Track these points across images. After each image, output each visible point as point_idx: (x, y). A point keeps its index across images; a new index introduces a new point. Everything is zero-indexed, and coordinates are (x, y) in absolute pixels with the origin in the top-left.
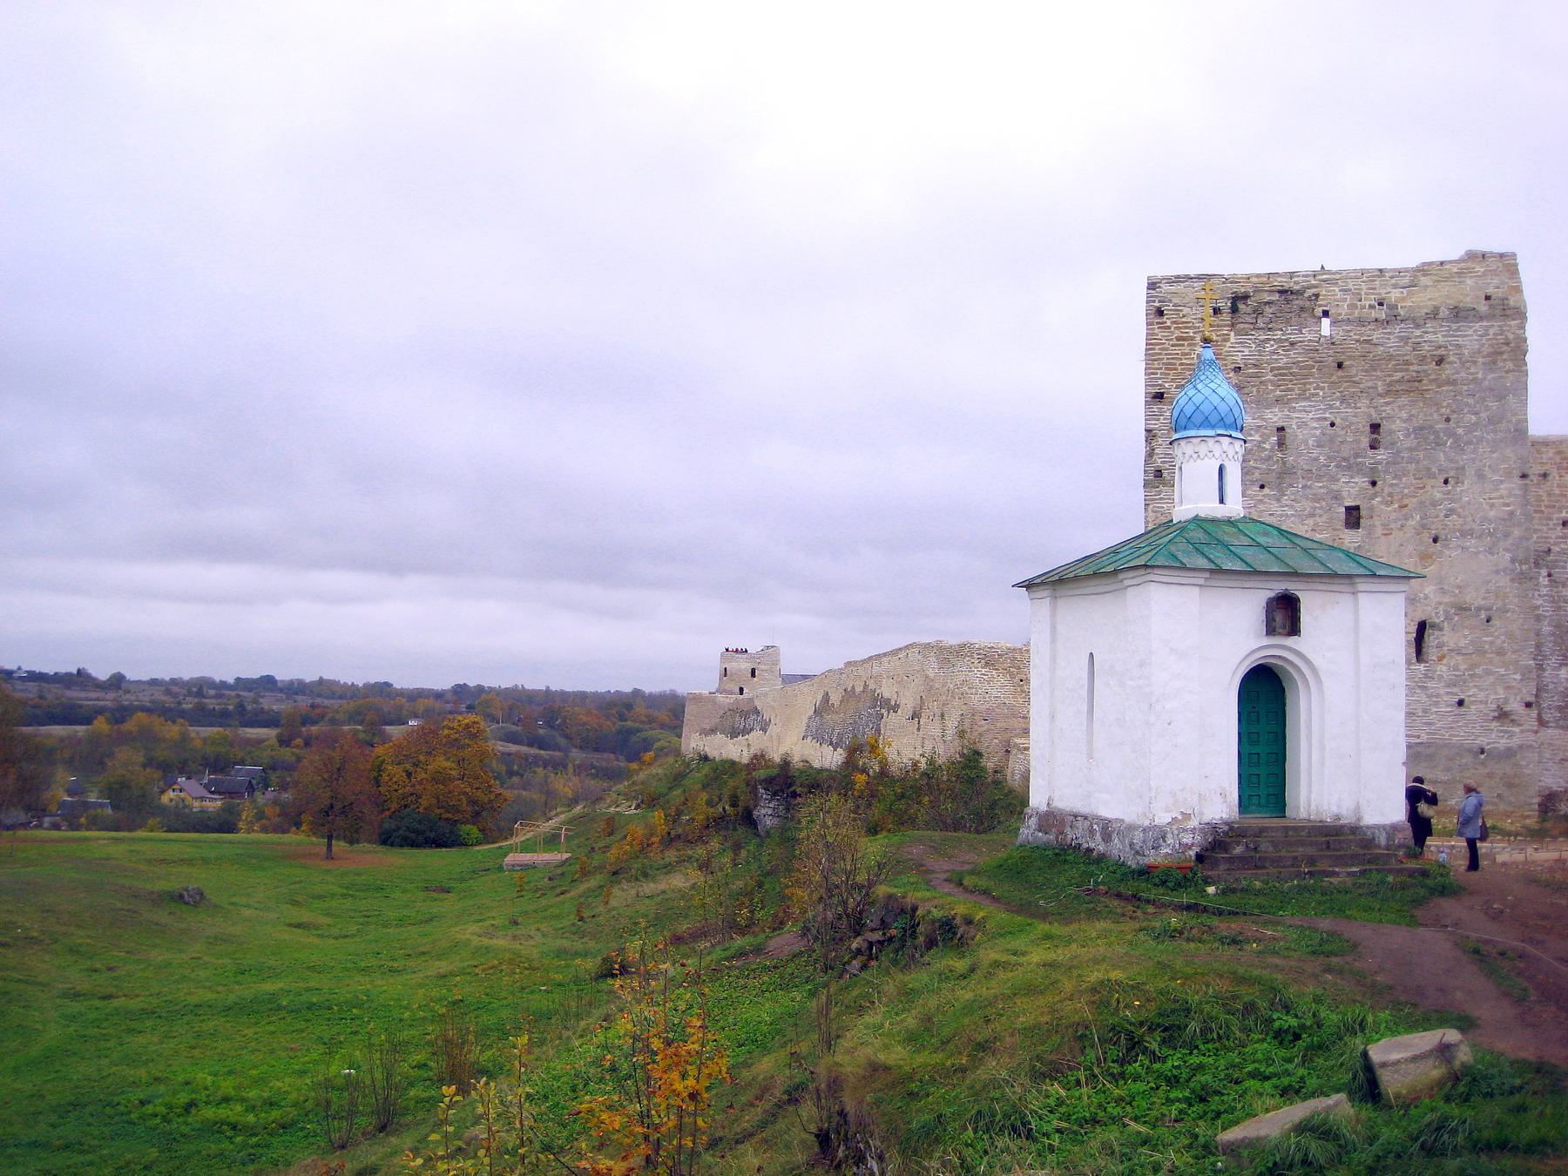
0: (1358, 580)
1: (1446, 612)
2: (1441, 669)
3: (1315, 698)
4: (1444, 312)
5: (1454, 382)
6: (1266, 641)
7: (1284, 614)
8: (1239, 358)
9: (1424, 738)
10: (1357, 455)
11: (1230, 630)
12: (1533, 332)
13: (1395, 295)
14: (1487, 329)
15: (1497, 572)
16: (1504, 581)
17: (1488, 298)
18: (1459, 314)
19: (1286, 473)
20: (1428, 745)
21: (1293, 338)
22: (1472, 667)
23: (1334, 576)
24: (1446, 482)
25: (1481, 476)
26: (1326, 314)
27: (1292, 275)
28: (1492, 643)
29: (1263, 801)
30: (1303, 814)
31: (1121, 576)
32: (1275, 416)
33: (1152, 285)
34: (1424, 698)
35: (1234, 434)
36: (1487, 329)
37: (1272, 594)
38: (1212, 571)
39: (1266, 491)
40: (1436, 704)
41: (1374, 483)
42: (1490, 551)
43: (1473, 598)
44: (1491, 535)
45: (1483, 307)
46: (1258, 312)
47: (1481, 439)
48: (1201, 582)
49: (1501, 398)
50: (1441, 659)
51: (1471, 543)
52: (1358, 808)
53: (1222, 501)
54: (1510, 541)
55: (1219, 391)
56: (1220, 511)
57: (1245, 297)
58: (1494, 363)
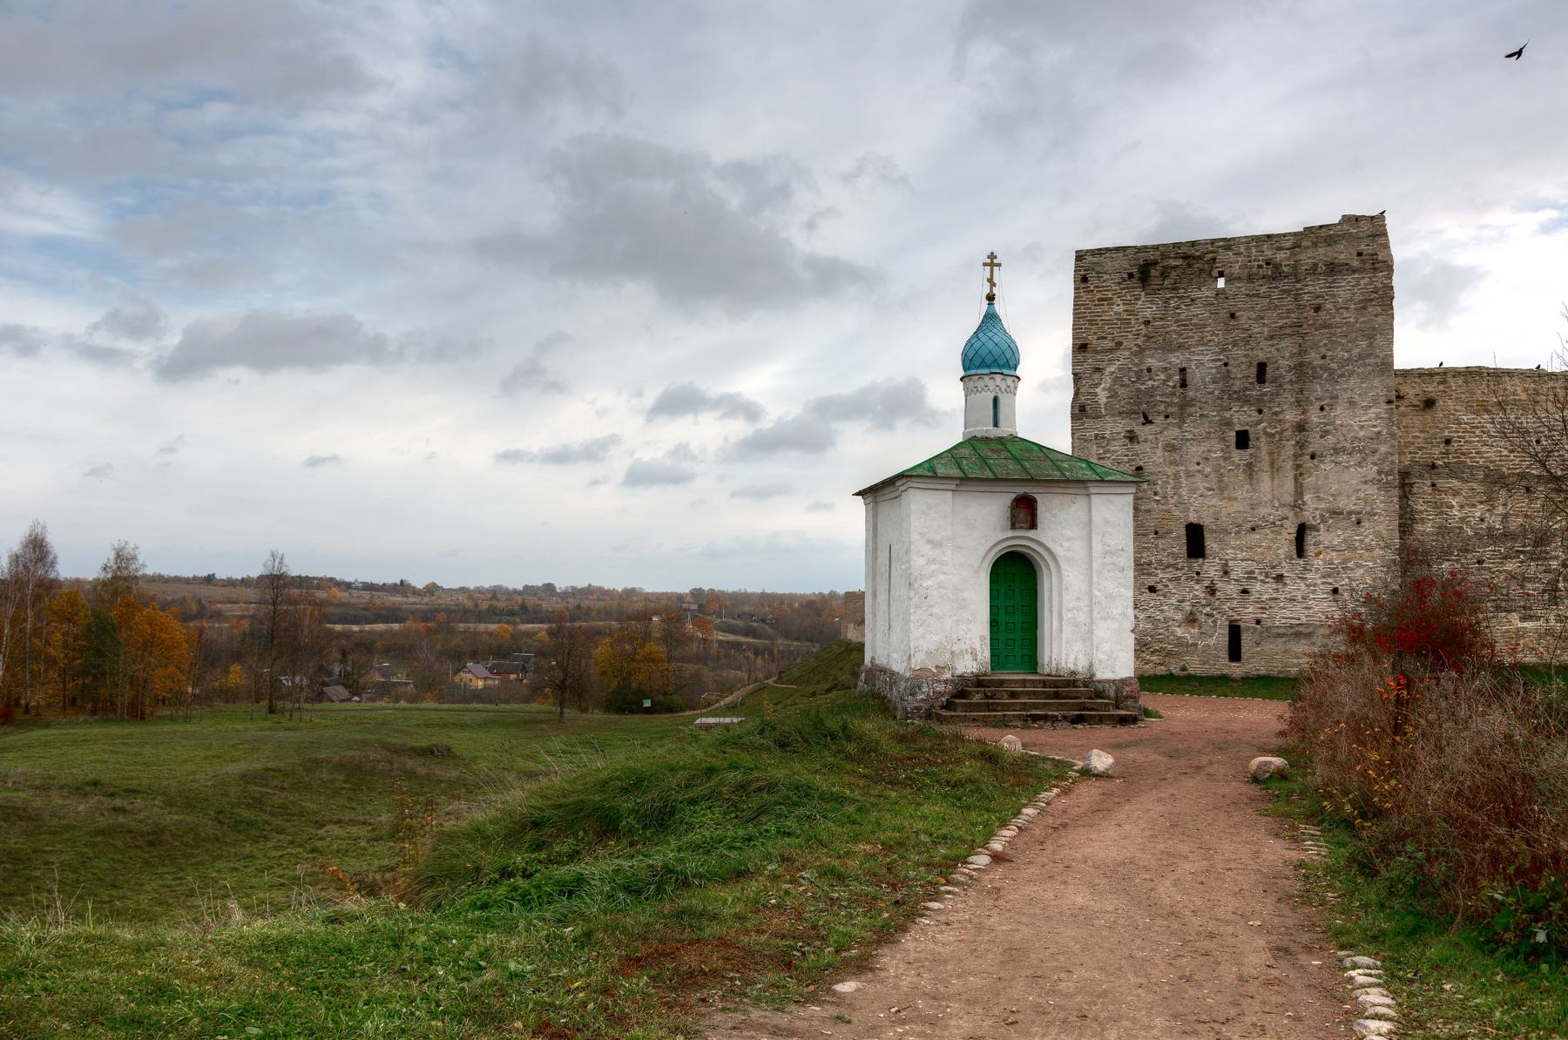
1: (1322, 516)
2: (1318, 563)
3: (1055, 579)
4: (1322, 268)
5: (1329, 327)
6: (1010, 534)
7: (1025, 512)
8: (1148, 314)
9: (1304, 620)
10: (1246, 389)
11: (980, 525)
12: (1396, 281)
13: (1280, 256)
14: (1358, 280)
15: (1366, 482)
16: (1372, 490)
17: (1360, 254)
18: (1333, 268)
19: (1185, 404)
20: (1308, 625)
21: (1194, 294)
22: (1345, 561)
23: (1068, 481)
24: (1322, 409)
25: (1352, 403)
26: (1221, 274)
27: (1193, 244)
28: (1361, 541)
29: (1019, 660)
30: (1047, 671)
32: (1176, 359)
33: (1080, 256)
34: (1303, 587)
35: (1006, 372)
36: (1358, 280)
38: (961, 479)
39: (1170, 420)
40: (1314, 592)
41: (1260, 412)
42: (1359, 464)
43: (1344, 504)
44: (1360, 452)
45: (1355, 264)
46: (1164, 275)
47: (1351, 373)
49: (1371, 337)
50: (1318, 554)
51: (1342, 458)
52: (1091, 665)
53: (996, 424)
54: (1377, 456)
56: (994, 433)
57: (1155, 263)
58: (1365, 308)
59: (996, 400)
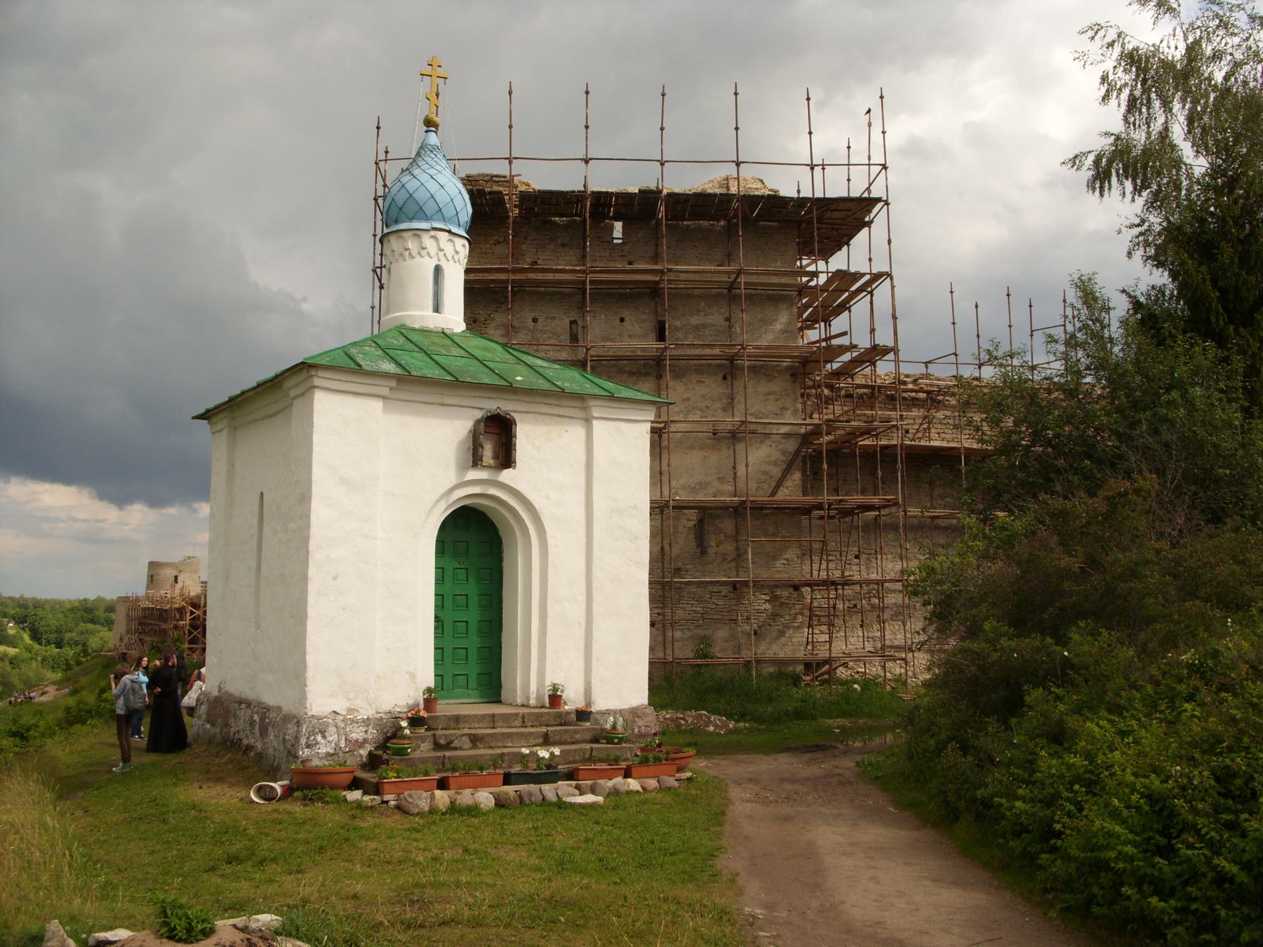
0: (592, 403)
31: (287, 385)
35: (454, 230)
37: (479, 415)
48: (386, 392)
53: (437, 309)
55: (439, 177)
59: (438, 270)
